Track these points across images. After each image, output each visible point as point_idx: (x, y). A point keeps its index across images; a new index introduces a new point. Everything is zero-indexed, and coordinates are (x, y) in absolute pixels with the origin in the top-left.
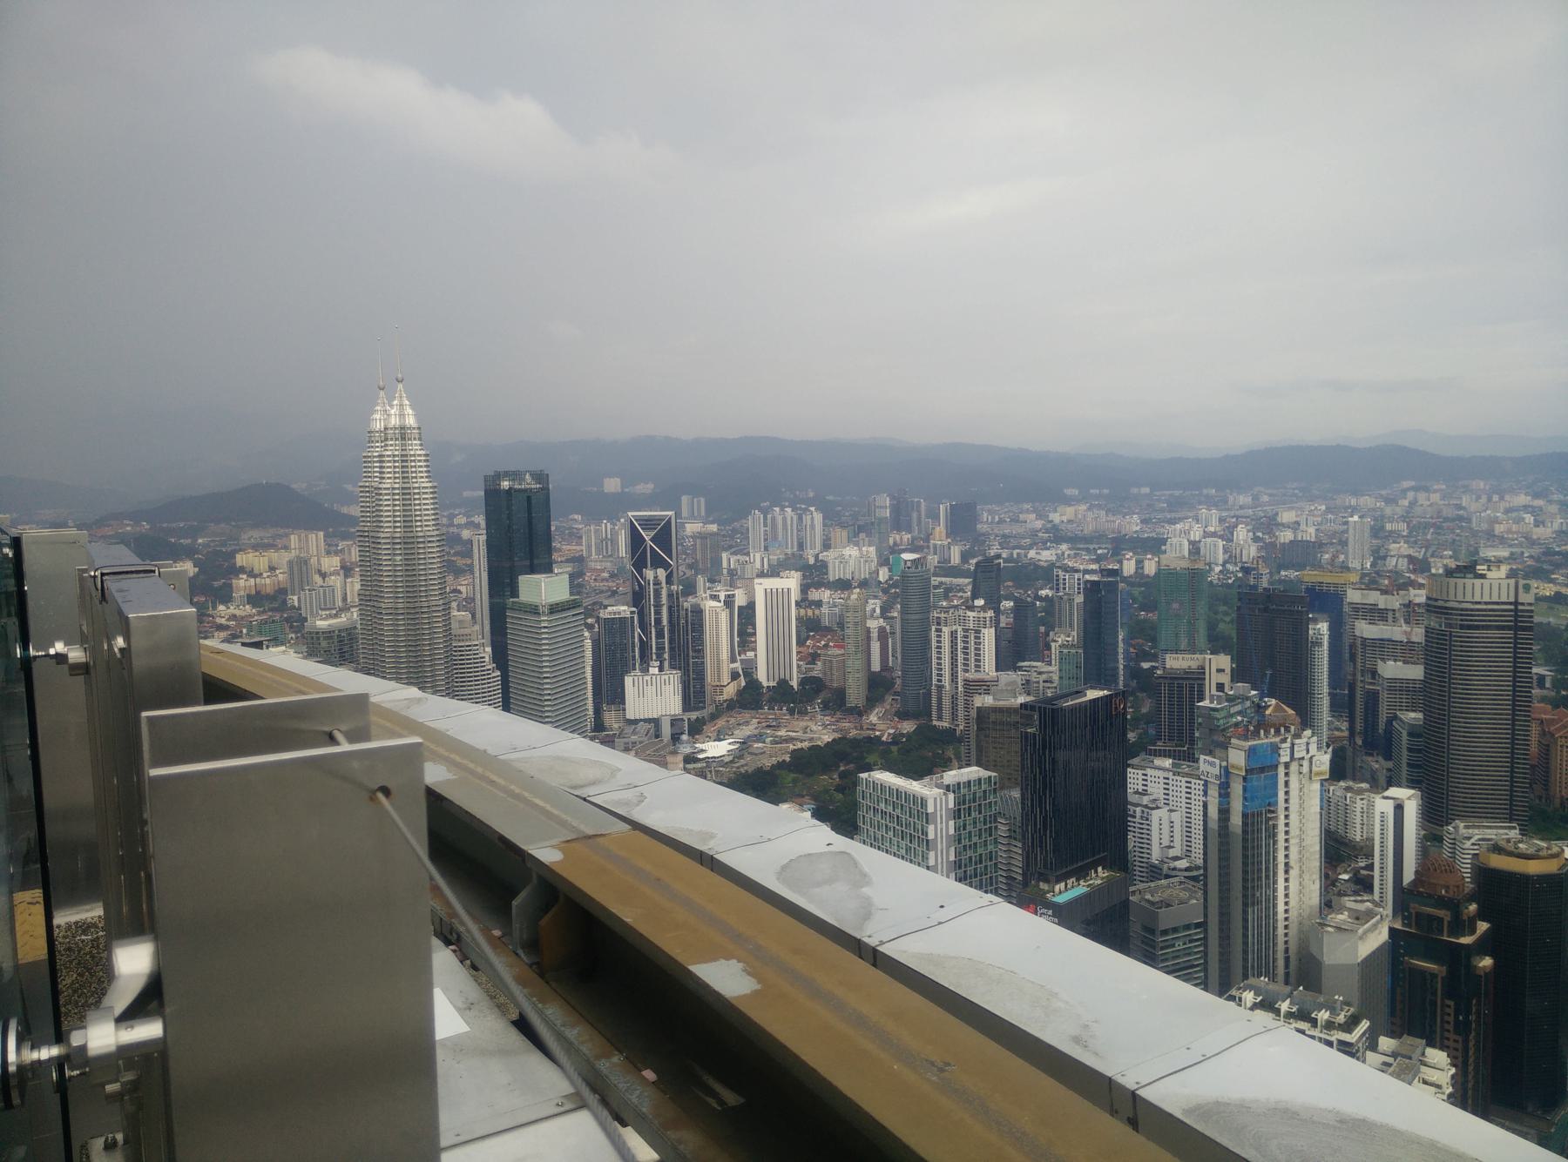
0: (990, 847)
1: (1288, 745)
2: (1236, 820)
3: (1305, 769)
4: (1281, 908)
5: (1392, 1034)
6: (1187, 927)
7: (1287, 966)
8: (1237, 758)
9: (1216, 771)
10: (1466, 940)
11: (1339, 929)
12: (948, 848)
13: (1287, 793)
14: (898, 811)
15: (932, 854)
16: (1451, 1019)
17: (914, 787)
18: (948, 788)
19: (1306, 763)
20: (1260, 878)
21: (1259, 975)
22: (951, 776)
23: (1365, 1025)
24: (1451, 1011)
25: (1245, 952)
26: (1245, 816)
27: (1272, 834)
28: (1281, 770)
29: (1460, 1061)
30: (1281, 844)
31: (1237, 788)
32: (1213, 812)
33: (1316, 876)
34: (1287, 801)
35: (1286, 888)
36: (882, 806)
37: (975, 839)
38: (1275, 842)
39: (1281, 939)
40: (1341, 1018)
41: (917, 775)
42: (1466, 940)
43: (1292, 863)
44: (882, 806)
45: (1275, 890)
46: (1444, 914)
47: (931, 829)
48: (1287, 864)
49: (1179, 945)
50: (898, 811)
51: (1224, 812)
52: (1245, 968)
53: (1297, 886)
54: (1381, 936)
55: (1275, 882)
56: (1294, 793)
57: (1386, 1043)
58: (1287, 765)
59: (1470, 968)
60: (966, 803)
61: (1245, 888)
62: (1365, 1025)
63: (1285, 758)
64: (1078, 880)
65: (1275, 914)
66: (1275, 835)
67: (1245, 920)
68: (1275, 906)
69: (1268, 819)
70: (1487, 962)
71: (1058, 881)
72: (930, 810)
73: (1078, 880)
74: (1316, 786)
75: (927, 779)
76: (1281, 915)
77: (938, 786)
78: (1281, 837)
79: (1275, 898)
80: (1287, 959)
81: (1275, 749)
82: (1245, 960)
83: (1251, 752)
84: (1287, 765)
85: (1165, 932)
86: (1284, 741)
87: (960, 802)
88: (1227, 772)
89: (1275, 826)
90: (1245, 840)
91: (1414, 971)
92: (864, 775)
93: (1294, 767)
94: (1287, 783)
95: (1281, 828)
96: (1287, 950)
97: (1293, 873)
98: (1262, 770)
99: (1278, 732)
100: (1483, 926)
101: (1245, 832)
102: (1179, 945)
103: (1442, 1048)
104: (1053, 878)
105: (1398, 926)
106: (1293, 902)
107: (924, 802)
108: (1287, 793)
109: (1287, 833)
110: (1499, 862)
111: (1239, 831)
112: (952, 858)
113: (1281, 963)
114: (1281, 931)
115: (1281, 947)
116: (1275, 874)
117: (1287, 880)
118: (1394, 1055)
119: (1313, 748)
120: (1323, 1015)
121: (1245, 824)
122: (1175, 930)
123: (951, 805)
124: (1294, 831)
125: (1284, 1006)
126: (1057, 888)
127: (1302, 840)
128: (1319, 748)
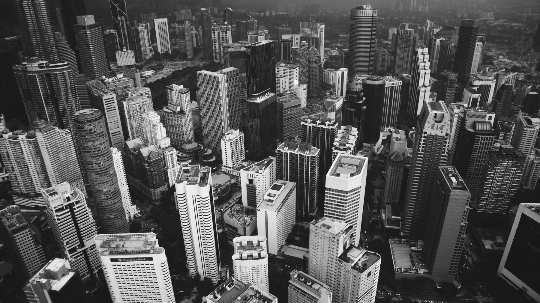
0: (237, 90)
6: (291, 107)
10: (361, 102)
15: (221, 93)
18: (224, 73)
22: (225, 70)
23: (337, 124)
41: (215, 71)
42: (361, 102)
57: (343, 127)
59: (361, 109)
62: (337, 124)
70: (365, 107)
72: (220, 80)
75: (218, 72)
77: (222, 73)
91: (348, 111)
92: (198, 72)
100: (364, 98)
107: (218, 78)
110: (369, 82)
118: (345, 130)
120: (328, 123)
122: (288, 108)
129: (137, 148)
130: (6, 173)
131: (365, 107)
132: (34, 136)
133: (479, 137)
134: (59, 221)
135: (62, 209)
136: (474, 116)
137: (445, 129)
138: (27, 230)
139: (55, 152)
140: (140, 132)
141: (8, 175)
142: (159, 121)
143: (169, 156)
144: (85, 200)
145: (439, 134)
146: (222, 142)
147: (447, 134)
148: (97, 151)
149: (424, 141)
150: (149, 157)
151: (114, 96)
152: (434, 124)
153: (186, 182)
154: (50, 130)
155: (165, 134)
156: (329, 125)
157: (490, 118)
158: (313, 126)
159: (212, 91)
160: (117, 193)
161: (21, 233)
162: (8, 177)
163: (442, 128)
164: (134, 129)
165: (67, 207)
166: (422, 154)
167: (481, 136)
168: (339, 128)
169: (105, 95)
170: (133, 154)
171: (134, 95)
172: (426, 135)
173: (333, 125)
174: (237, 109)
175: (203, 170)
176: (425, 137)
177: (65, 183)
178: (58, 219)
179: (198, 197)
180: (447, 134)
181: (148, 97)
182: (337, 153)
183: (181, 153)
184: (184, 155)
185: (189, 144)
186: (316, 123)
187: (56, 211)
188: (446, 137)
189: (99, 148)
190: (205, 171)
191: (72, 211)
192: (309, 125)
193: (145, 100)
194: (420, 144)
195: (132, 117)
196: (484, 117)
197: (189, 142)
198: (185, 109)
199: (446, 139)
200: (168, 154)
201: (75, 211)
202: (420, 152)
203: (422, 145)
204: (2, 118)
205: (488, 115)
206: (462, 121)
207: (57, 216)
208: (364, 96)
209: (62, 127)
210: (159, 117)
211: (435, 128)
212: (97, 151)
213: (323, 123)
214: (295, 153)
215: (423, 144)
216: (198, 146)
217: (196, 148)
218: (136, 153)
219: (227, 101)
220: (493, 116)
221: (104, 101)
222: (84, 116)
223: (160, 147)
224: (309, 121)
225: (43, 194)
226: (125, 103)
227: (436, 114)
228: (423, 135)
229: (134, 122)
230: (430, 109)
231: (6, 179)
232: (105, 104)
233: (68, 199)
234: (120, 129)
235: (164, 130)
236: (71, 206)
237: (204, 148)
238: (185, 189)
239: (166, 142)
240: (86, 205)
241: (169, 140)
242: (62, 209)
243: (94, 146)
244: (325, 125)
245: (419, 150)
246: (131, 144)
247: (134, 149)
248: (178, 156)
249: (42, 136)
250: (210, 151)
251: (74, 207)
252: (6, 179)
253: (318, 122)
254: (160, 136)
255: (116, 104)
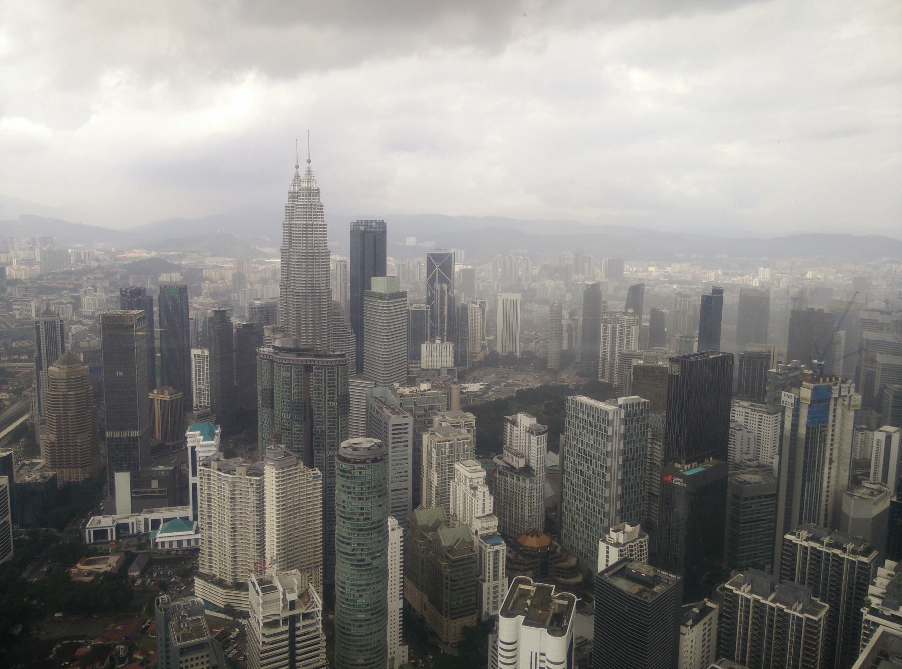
0: (643, 443)
1: (838, 387)
2: (802, 431)
3: (846, 403)
4: (825, 484)
6: (759, 497)
7: (826, 519)
8: (806, 393)
9: (792, 401)
11: (861, 498)
12: (620, 441)
13: (834, 416)
14: (590, 419)
17: (601, 405)
18: (621, 406)
19: (847, 399)
20: (814, 466)
21: (809, 522)
22: (621, 401)
23: (875, 553)
25: (801, 509)
26: (808, 428)
27: (824, 441)
28: (832, 403)
30: (828, 447)
31: (804, 412)
32: (788, 425)
33: (847, 468)
34: (834, 421)
35: (829, 473)
36: (581, 415)
37: (635, 438)
38: (825, 446)
39: (823, 503)
40: (861, 548)
43: (834, 458)
44: (581, 415)
45: (822, 474)
47: (610, 430)
48: (831, 459)
49: (754, 507)
50: (590, 419)
51: (795, 426)
52: (801, 518)
53: (834, 474)
54: (885, 505)
55: (823, 469)
56: (839, 417)
58: (836, 400)
60: (632, 416)
61: (804, 471)
62: (875, 553)
63: (835, 395)
64: (698, 463)
65: (821, 487)
66: (825, 441)
67: (803, 490)
68: (822, 483)
69: (822, 432)
71: (686, 463)
72: (611, 418)
73: (698, 463)
74: (852, 414)
76: (825, 489)
78: (829, 442)
79: (822, 478)
80: (826, 515)
81: (830, 389)
82: (801, 514)
83: (815, 391)
84: (836, 400)
85: (745, 499)
86: (836, 385)
87: (628, 415)
88: (798, 402)
89: (826, 436)
90: (807, 443)
92: (570, 398)
93: (840, 401)
94: (835, 411)
95: (829, 437)
96: (826, 510)
97: (835, 465)
98: (820, 402)
99: (831, 380)
101: (807, 438)
102: (754, 507)
104: (683, 461)
105: (895, 499)
106: (832, 482)
108: (834, 416)
109: (832, 440)
111: (804, 438)
112: (621, 447)
113: (822, 517)
114: (824, 498)
115: (823, 507)
116: (823, 464)
117: (830, 468)
119: (853, 390)
121: (807, 433)
122: (752, 498)
123: (623, 416)
124: (837, 439)
125: (826, 540)
126: (686, 467)
127: (841, 445)
128: (857, 391)
129: (435, 528)
130: (197, 532)
132: (260, 473)
134: (264, 648)
135: (275, 624)
138: (205, 654)
139: (287, 509)
140: (444, 495)
141: (198, 536)
142: (481, 480)
143: (491, 555)
144: (320, 615)
146: (602, 546)
148: (365, 519)
150: (450, 550)
151: (410, 420)
153: (521, 618)
154: (290, 466)
155: (489, 509)
158: (813, 548)
159: (592, 438)
160: (380, 611)
161: (194, 657)
162: (197, 540)
164: (434, 489)
165: (285, 620)
169: (393, 417)
170: (423, 537)
171: (444, 424)
173: (866, 553)
174: (638, 480)
175: (559, 598)
177: (294, 571)
178: (263, 643)
179: (543, 658)
181: (469, 431)
182: (877, 625)
183: (514, 553)
184: (520, 558)
185: (532, 536)
186: (822, 543)
187: (266, 625)
189: (368, 514)
190: (565, 603)
191: (293, 630)
192: (805, 544)
193: (462, 437)
195: (434, 466)
197: (534, 533)
198: (533, 464)
200: (489, 550)
201: (298, 633)
204: (217, 432)
207: (263, 635)
209: (311, 465)
210: (484, 474)
212: (365, 519)
213: (837, 546)
214: (768, 603)
216: (550, 545)
217: (545, 547)
218: (430, 536)
219: (621, 462)
221: (391, 428)
222: (355, 449)
223: (476, 532)
224: (804, 534)
225: (250, 586)
226: (426, 438)
229: (436, 475)
231: (193, 543)
232: (391, 432)
233: (293, 605)
234: (409, 484)
235: (489, 501)
236: (293, 620)
237: (563, 550)
238: (517, 631)
239: (489, 524)
240: (320, 626)
241: (495, 522)
242: (275, 624)
243: (362, 509)
244: (845, 550)
246: (423, 516)
247: (427, 528)
248: (508, 558)
249: (274, 474)
250: (573, 561)
251: (298, 625)
252: (193, 543)
253: (826, 540)
254: (480, 510)
255: (410, 437)
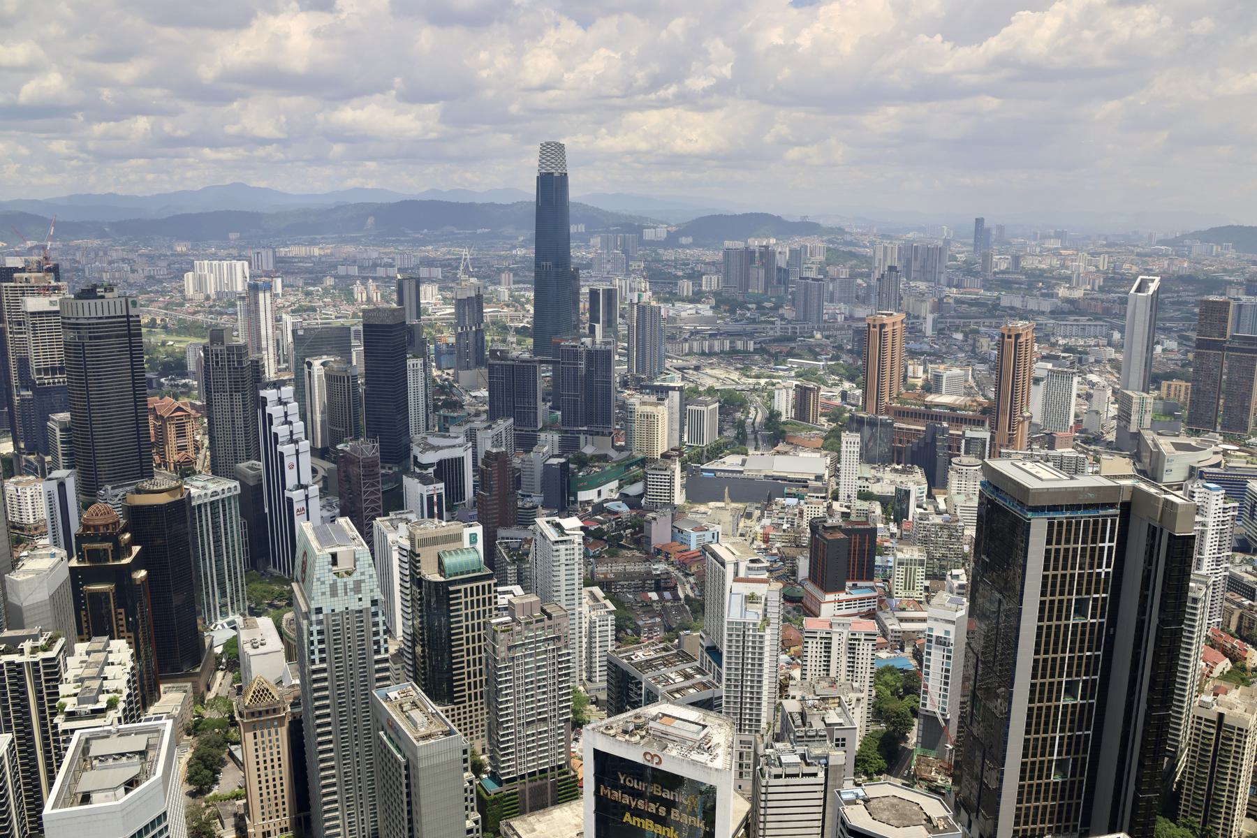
5: (82, 641)
16: (124, 622)
24: (122, 616)
29: (135, 644)
46: (108, 545)
57: (81, 648)
70: (143, 573)
100: (136, 549)
103: (119, 638)
105: (74, 563)
131: (143, 573)
133: (459, 591)
136: (434, 541)
137: (365, 587)
145: (355, 606)
147: (374, 603)
149: (320, 632)
152: (335, 583)
156: (34, 650)
157: (473, 538)
163: (357, 588)
166: (324, 670)
167: (462, 587)
168: (68, 651)
172: (321, 617)
176: (320, 622)
180: (374, 603)
182: (73, 731)
188: (373, 609)
194: (312, 643)
196: (458, 537)
199: (375, 614)
202: (318, 666)
203: (317, 647)
205: (467, 532)
206: (413, 558)
208: (134, 542)
211: (340, 591)
215: (321, 642)
220: (478, 530)
227: (334, 556)
228: (314, 618)
230: (315, 544)
245: (313, 662)
